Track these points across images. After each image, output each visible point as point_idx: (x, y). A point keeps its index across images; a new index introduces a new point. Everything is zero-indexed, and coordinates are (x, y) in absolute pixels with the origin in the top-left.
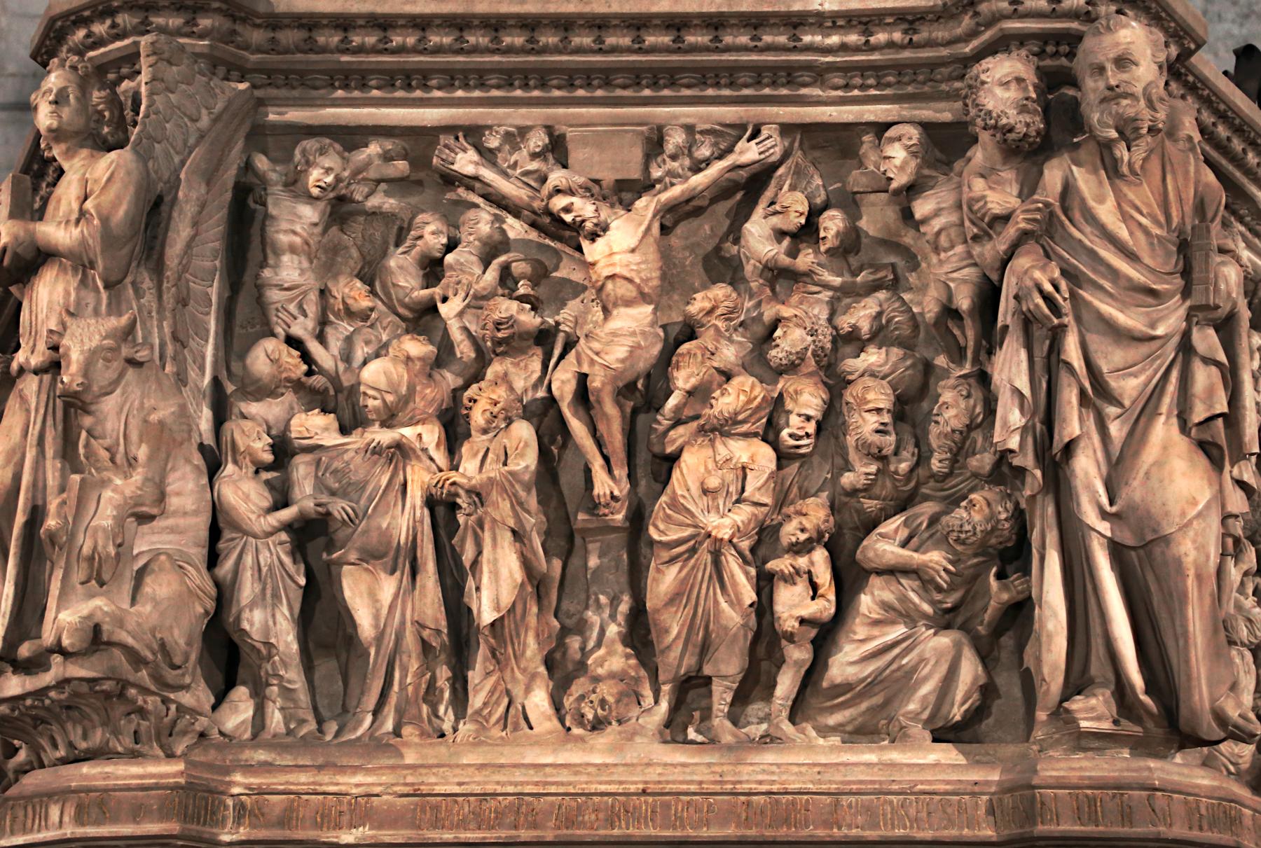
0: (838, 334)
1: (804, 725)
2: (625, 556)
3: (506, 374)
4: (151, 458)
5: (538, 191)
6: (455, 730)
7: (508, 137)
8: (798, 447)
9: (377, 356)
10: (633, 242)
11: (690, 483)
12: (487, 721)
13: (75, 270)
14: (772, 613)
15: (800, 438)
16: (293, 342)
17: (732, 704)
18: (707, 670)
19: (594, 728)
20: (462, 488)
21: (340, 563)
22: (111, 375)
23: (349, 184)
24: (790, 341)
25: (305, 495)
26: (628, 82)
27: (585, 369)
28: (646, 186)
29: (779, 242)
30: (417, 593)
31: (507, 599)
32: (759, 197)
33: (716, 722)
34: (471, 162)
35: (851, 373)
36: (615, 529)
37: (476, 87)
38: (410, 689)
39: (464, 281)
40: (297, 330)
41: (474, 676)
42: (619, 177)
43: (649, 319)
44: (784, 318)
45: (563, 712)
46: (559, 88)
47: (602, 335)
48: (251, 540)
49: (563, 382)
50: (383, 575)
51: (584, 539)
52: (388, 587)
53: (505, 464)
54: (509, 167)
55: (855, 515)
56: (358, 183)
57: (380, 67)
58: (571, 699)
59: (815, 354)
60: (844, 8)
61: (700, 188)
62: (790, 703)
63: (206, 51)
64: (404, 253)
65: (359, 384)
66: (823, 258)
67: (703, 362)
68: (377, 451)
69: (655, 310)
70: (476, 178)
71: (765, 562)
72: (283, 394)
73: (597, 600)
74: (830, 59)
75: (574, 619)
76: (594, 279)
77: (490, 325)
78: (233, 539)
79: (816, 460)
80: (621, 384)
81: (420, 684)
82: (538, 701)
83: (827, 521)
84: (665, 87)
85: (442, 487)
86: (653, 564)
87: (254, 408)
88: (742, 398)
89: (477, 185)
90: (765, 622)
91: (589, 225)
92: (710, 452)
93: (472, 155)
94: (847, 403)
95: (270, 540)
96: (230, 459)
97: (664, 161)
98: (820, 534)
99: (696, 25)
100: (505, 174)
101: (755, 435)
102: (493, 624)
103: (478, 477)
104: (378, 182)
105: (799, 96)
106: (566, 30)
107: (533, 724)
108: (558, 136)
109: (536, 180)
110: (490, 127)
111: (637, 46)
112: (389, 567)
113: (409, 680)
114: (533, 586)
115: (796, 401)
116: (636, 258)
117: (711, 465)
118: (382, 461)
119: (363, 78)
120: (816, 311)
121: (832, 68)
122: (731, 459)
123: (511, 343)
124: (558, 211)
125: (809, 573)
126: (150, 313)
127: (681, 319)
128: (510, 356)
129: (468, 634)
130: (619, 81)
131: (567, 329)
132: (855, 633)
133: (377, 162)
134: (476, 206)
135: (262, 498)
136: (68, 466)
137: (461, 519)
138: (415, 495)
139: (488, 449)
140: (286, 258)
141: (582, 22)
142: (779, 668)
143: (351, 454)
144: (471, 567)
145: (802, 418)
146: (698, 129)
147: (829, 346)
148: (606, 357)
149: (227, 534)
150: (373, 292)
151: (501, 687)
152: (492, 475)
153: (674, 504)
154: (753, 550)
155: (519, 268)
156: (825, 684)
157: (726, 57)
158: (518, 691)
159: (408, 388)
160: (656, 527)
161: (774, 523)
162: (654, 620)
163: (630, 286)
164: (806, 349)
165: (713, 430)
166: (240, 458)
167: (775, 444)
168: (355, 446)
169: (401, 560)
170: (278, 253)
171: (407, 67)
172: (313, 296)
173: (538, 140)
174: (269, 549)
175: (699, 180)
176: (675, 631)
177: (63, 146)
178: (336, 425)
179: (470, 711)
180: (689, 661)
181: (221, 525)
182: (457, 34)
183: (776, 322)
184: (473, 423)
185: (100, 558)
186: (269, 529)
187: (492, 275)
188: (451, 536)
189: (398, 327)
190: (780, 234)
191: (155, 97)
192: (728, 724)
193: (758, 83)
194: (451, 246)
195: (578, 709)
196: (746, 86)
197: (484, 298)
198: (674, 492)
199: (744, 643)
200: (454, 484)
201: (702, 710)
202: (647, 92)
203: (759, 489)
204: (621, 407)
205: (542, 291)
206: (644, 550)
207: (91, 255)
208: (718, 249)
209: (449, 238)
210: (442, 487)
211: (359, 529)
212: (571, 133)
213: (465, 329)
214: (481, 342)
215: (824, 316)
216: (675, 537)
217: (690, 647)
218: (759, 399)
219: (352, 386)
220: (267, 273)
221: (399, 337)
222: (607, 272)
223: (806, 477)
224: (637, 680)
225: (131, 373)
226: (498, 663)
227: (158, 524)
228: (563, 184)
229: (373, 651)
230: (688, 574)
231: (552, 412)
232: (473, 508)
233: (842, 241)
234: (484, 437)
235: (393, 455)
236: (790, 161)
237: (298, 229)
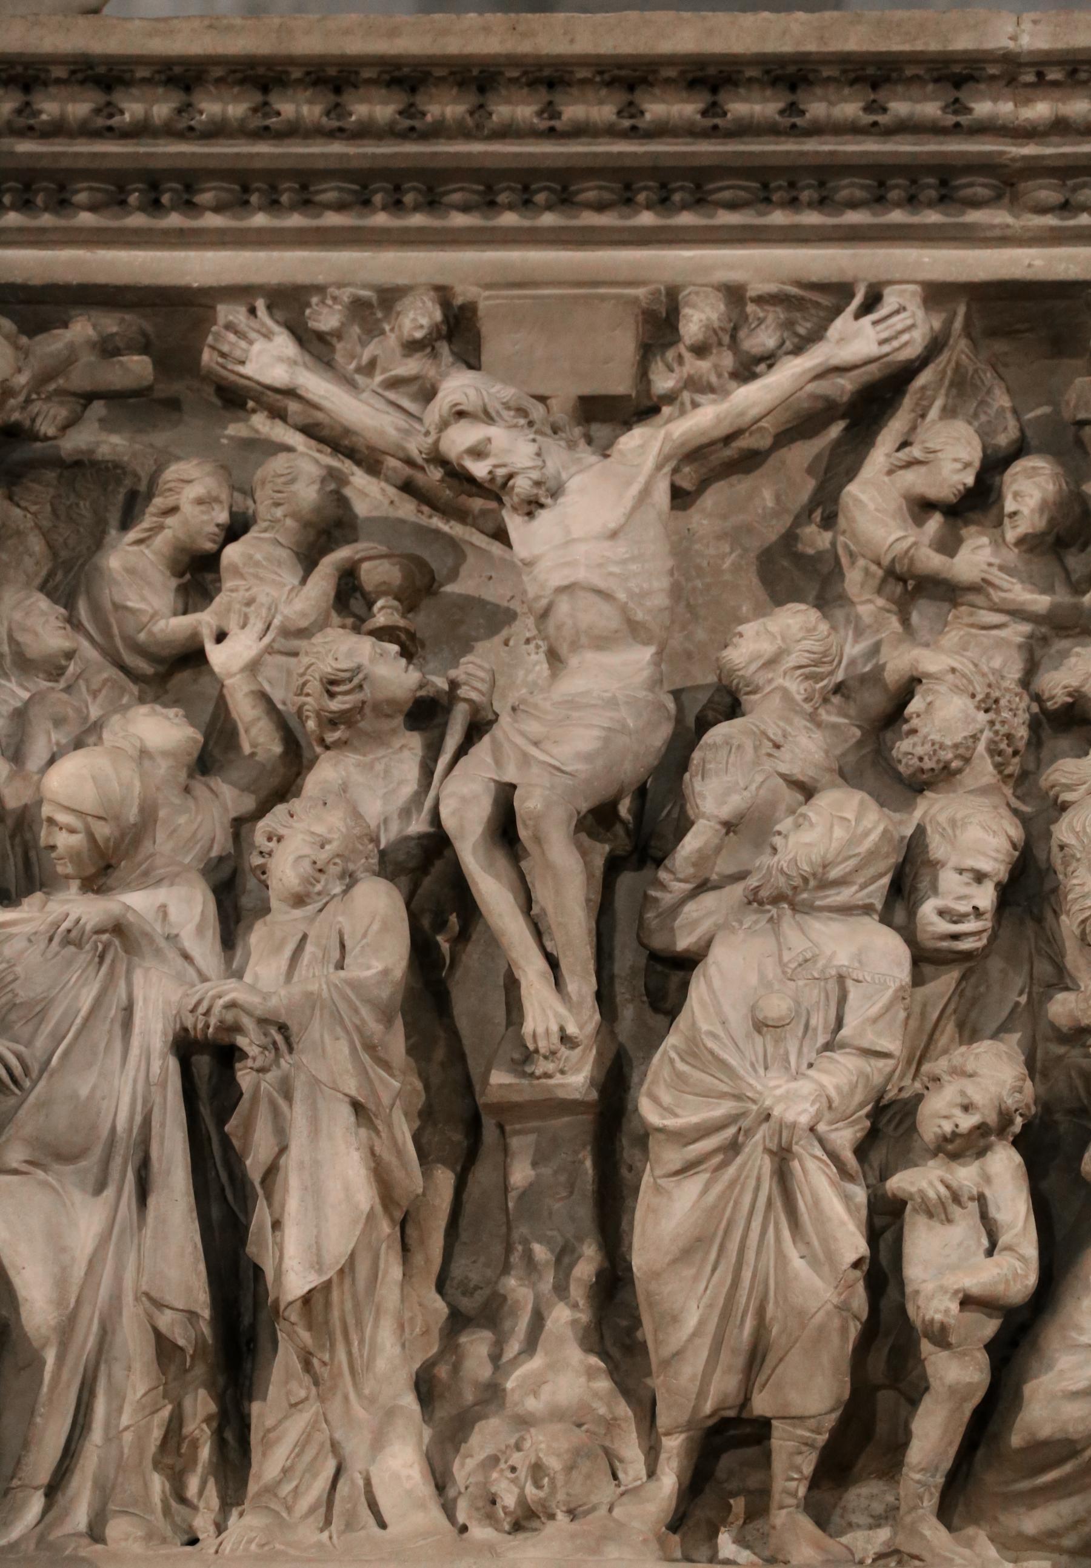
0: (1043, 710)
1: (971, 1531)
3: (344, 788)
5: (420, 420)
6: (220, 1528)
7: (359, 309)
8: (955, 937)
9: (78, 744)
10: (612, 517)
11: (727, 1009)
12: (289, 1509)
14: (901, 1284)
15: (960, 918)
17: (815, 1482)
18: (761, 1405)
19: (517, 1527)
20: (249, 1014)
23: (28, 401)
24: (944, 718)
26: (607, 196)
28: (643, 409)
29: (919, 521)
30: (148, 1231)
31: (339, 1243)
32: (876, 433)
33: (779, 1517)
34: (281, 359)
35: (1069, 788)
37: (293, 207)
38: (128, 1437)
39: (262, 599)
41: (262, 1413)
42: (588, 390)
43: (646, 674)
44: (929, 676)
45: (451, 1493)
46: (465, 208)
47: (547, 705)
49: (464, 800)
50: (77, 1196)
51: (501, 1127)
52: (87, 1220)
53: (340, 966)
54: (359, 370)
55: (1079, 1083)
56: (48, 399)
57: (95, 165)
58: (471, 1463)
59: (993, 751)
60: (1060, 45)
61: (754, 412)
62: (940, 1480)
64: (140, 542)
65: (39, 803)
66: (1012, 556)
67: (756, 763)
68: (73, 939)
69: (659, 653)
70: (290, 393)
71: (884, 1177)
73: (528, 1256)
74: (1030, 150)
75: (479, 1297)
76: (532, 591)
77: (315, 686)
79: (995, 965)
80: (584, 807)
81: (149, 1430)
82: (399, 1466)
83: (1020, 1090)
84: (684, 207)
86: (646, 1179)
88: (839, 833)
89: (293, 406)
90: (885, 1304)
91: (522, 485)
92: (771, 944)
93: (283, 344)
94: (1062, 848)
97: (680, 359)
98: (1005, 1119)
99: (750, 80)
100: (350, 383)
101: (867, 909)
102: (307, 1300)
103: (283, 992)
104: (89, 398)
105: (965, 226)
106: (482, 90)
107: (387, 1517)
108: (462, 308)
109: (414, 398)
110: (320, 289)
111: (627, 123)
112: (91, 1179)
113: (125, 1420)
114: (392, 1219)
115: (952, 841)
116: (621, 549)
117: (772, 971)
118: (84, 957)
119: (62, 188)
120: (997, 663)
121: (1035, 169)
122: (814, 959)
123: (352, 722)
124: (460, 457)
125: (981, 1199)
127: (712, 679)
128: (355, 750)
129: (253, 1326)
130: (591, 195)
131: (474, 696)
132: (1081, 1330)
133: (88, 358)
134: (289, 449)
137: (245, 1078)
138: (153, 1030)
139: (305, 937)
141: (514, 73)
142: (914, 1403)
143: (19, 944)
144: (263, 1181)
145: (967, 877)
146: (751, 293)
147: (1023, 732)
148: (555, 750)
150: (73, 622)
151: (322, 1436)
152: (314, 987)
153: (694, 1052)
154: (861, 1150)
155: (376, 573)
156: (1016, 1440)
157: (810, 145)
158: (356, 1447)
159: (142, 810)
160: (655, 1100)
161: (905, 1095)
162: (649, 1295)
163: (606, 608)
164: (975, 738)
165: (777, 899)
167: (909, 934)
168: (28, 928)
171: (152, 164)
173: (419, 317)
175: (754, 397)
176: (691, 1321)
179: (253, 1488)
180: (724, 1385)
182: (258, 97)
183: (911, 685)
184: (273, 883)
187: (323, 580)
188: (223, 1115)
189: (123, 690)
190: (922, 507)
192: (806, 1524)
193: (879, 200)
194: (236, 529)
195: (485, 1485)
196: (853, 205)
197: (303, 633)
198: (694, 1023)
199: (839, 1347)
200: (232, 1005)
201: (747, 1492)
202: (647, 219)
203: (875, 1020)
204: (584, 853)
205: (422, 622)
206: (628, 1152)
208: (790, 538)
209: (232, 514)
210: (207, 1013)
213: (264, 698)
214: (293, 723)
215: (1014, 671)
216: (694, 1119)
217: (725, 1357)
218: (874, 837)
219: (26, 807)
221: (125, 708)
222: (557, 579)
223: (974, 1002)
224: (611, 1425)
226: (316, 1383)
228: (470, 400)
229: (50, 1357)
230: (724, 1197)
231: (439, 866)
232: (270, 1055)
233: (1052, 521)
234: (298, 913)
235: (107, 946)
236: (943, 358)
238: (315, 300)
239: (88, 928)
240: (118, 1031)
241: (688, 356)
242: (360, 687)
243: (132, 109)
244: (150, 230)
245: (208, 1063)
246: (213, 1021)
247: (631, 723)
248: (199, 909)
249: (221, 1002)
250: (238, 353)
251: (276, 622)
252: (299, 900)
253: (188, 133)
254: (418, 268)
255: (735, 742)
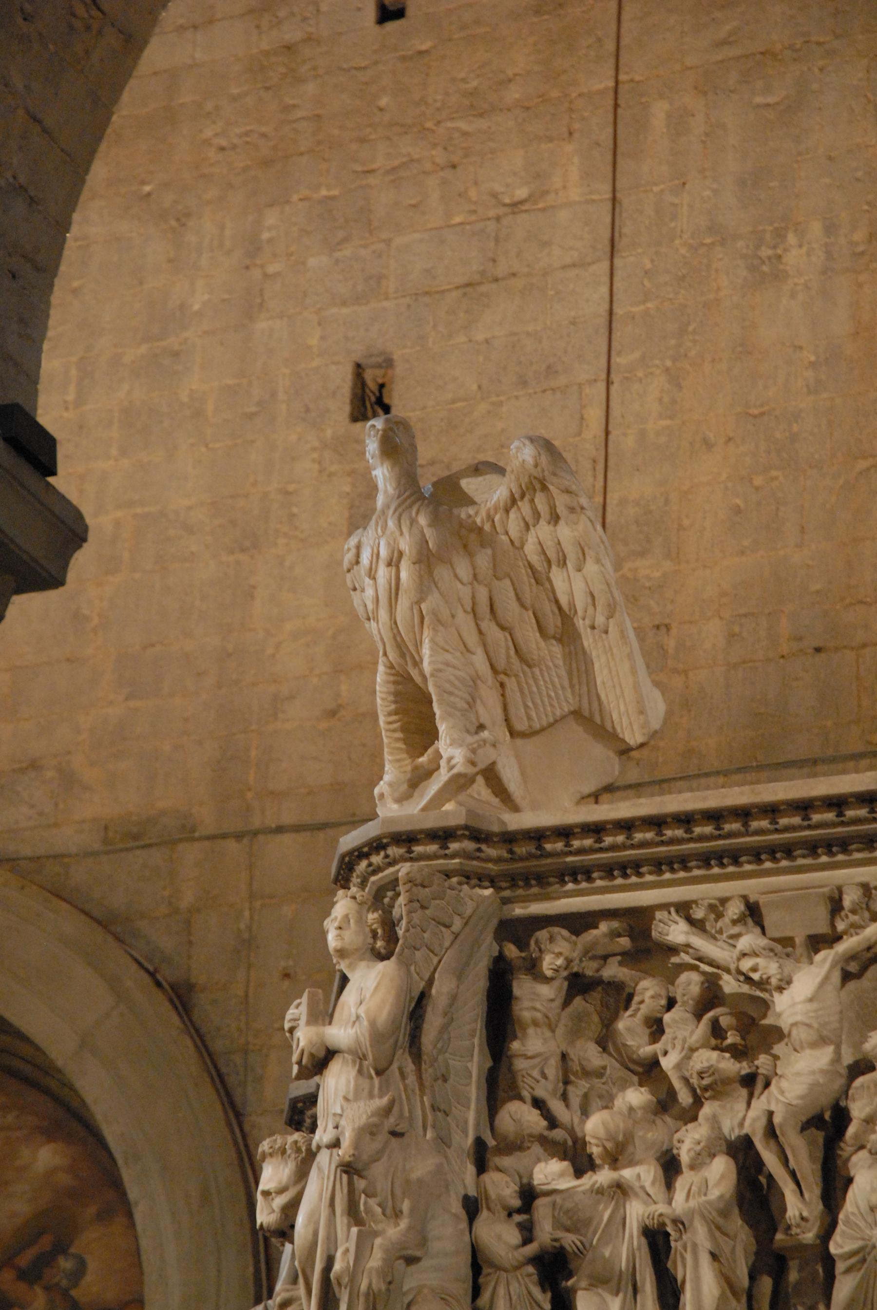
2: (821, 1271)
4: (412, 1211)
7: (712, 908)
13: (354, 1062)
16: (538, 1104)
21: (573, 1291)
22: (376, 1145)
25: (546, 1231)
27: (773, 1108)
34: (682, 932)
36: (806, 1247)
40: (540, 1093)
48: (503, 1273)
53: (705, 1195)
56: (590, 959)
63: (458, 867)
68: (600, 1191)
72: (529, 1148)
77: (695, 1075)
78: (489, 1274)
85: (653, 1219)
87: (506, 1161)
95: (518, 1273)
96: (484, 1206)
97: (847, 917)
110: (695, 902)
123: (712, 1088)
126: (413, 1091)
135: (513, 1236)
136: (352, 1221)
137: (673, 1244)
138: (633, 1226)
140: (531, 1031)
149: (486, 1270)
153: (847, 1222)
159: (624, 1135)
166: (492, 1205)
169: (623, 1283)
170: (524, 1029)
172: (553, 1063)
173: (735, 909)
174: (519, 1282)
177: (347, 961)
178: (571, 1170)
181: (480, 1263)
185: (374, 1294)
186: (516, 1263)
191: (413, 914)
200: (661, 1215)
207: (364, 1049)
211: (587, 1259)
212: (762, 900)
220: (515, 1045)
222: (791, 1020)
225: (394, 1141)
227: (424, 1263)
237: (538, 1005)
238: (694, 906)
239: (605, 1187)
240: (621, 1226)
241: (850, 914)
242: (713, 1074)
243: (608, 840)
244: (625, 885)
245: (658, 1241)
246: (656, 1221)
247: (821, 1081)
248: (652, 1174)
249: (657, 1214)
250: (665, 931)
251: (686, 1046)
252: (692, 1167)
253: (633, 847)
254: (734, 888)
255: (865, 1085)
